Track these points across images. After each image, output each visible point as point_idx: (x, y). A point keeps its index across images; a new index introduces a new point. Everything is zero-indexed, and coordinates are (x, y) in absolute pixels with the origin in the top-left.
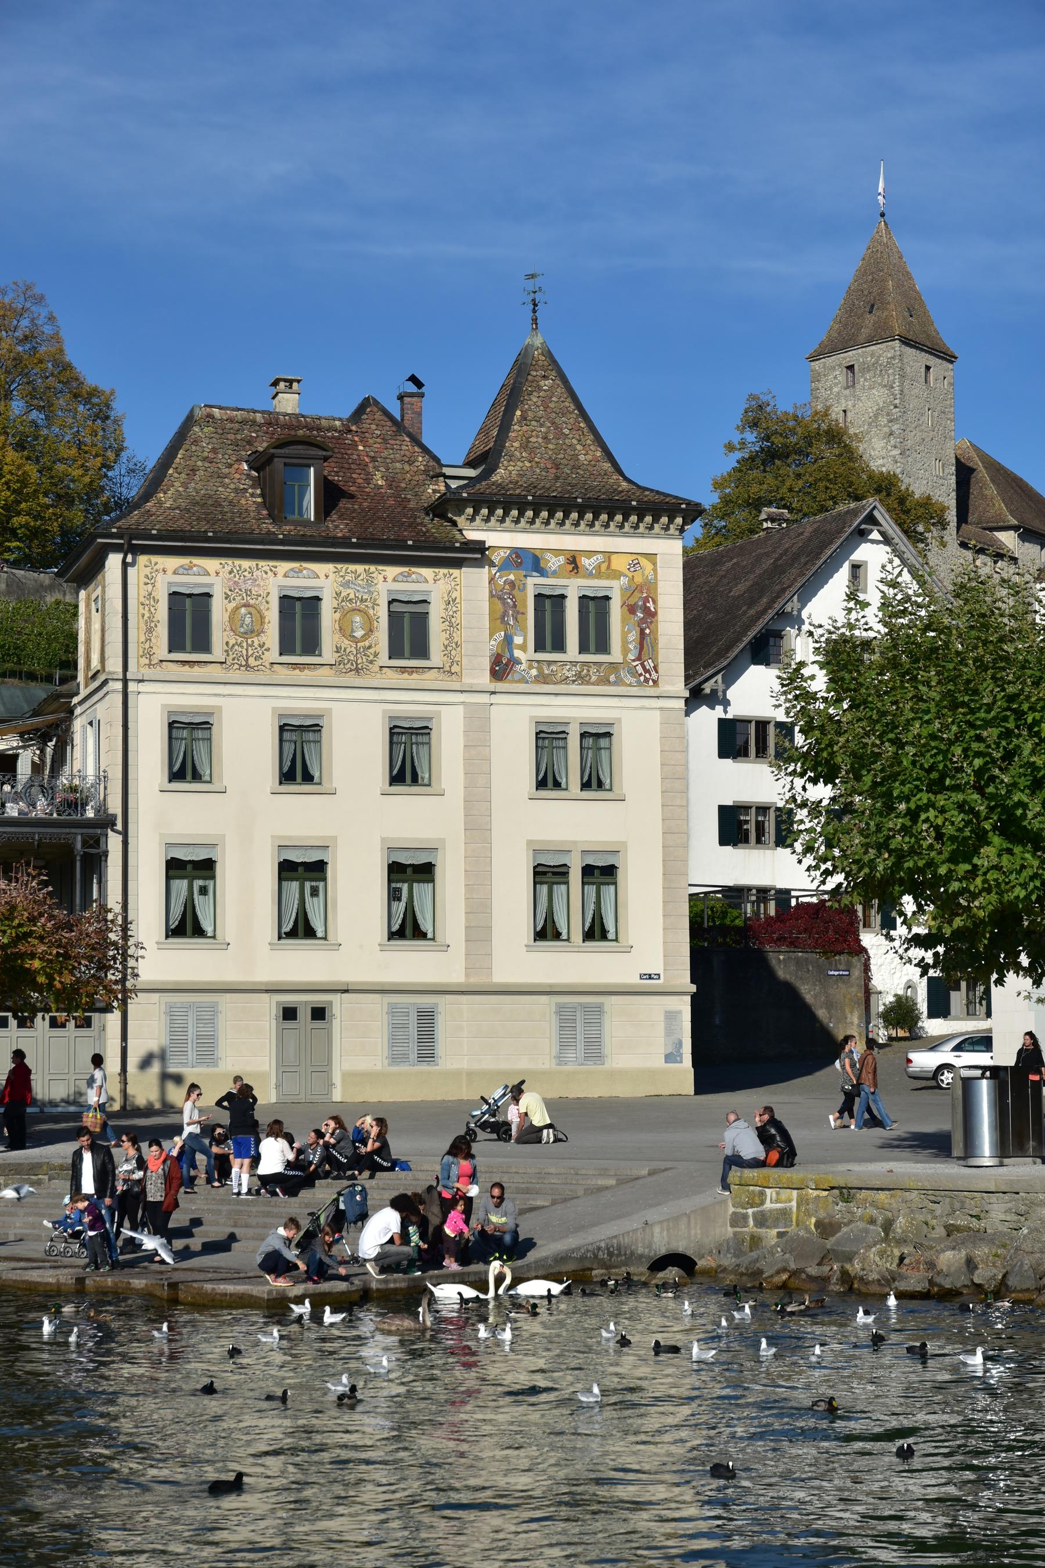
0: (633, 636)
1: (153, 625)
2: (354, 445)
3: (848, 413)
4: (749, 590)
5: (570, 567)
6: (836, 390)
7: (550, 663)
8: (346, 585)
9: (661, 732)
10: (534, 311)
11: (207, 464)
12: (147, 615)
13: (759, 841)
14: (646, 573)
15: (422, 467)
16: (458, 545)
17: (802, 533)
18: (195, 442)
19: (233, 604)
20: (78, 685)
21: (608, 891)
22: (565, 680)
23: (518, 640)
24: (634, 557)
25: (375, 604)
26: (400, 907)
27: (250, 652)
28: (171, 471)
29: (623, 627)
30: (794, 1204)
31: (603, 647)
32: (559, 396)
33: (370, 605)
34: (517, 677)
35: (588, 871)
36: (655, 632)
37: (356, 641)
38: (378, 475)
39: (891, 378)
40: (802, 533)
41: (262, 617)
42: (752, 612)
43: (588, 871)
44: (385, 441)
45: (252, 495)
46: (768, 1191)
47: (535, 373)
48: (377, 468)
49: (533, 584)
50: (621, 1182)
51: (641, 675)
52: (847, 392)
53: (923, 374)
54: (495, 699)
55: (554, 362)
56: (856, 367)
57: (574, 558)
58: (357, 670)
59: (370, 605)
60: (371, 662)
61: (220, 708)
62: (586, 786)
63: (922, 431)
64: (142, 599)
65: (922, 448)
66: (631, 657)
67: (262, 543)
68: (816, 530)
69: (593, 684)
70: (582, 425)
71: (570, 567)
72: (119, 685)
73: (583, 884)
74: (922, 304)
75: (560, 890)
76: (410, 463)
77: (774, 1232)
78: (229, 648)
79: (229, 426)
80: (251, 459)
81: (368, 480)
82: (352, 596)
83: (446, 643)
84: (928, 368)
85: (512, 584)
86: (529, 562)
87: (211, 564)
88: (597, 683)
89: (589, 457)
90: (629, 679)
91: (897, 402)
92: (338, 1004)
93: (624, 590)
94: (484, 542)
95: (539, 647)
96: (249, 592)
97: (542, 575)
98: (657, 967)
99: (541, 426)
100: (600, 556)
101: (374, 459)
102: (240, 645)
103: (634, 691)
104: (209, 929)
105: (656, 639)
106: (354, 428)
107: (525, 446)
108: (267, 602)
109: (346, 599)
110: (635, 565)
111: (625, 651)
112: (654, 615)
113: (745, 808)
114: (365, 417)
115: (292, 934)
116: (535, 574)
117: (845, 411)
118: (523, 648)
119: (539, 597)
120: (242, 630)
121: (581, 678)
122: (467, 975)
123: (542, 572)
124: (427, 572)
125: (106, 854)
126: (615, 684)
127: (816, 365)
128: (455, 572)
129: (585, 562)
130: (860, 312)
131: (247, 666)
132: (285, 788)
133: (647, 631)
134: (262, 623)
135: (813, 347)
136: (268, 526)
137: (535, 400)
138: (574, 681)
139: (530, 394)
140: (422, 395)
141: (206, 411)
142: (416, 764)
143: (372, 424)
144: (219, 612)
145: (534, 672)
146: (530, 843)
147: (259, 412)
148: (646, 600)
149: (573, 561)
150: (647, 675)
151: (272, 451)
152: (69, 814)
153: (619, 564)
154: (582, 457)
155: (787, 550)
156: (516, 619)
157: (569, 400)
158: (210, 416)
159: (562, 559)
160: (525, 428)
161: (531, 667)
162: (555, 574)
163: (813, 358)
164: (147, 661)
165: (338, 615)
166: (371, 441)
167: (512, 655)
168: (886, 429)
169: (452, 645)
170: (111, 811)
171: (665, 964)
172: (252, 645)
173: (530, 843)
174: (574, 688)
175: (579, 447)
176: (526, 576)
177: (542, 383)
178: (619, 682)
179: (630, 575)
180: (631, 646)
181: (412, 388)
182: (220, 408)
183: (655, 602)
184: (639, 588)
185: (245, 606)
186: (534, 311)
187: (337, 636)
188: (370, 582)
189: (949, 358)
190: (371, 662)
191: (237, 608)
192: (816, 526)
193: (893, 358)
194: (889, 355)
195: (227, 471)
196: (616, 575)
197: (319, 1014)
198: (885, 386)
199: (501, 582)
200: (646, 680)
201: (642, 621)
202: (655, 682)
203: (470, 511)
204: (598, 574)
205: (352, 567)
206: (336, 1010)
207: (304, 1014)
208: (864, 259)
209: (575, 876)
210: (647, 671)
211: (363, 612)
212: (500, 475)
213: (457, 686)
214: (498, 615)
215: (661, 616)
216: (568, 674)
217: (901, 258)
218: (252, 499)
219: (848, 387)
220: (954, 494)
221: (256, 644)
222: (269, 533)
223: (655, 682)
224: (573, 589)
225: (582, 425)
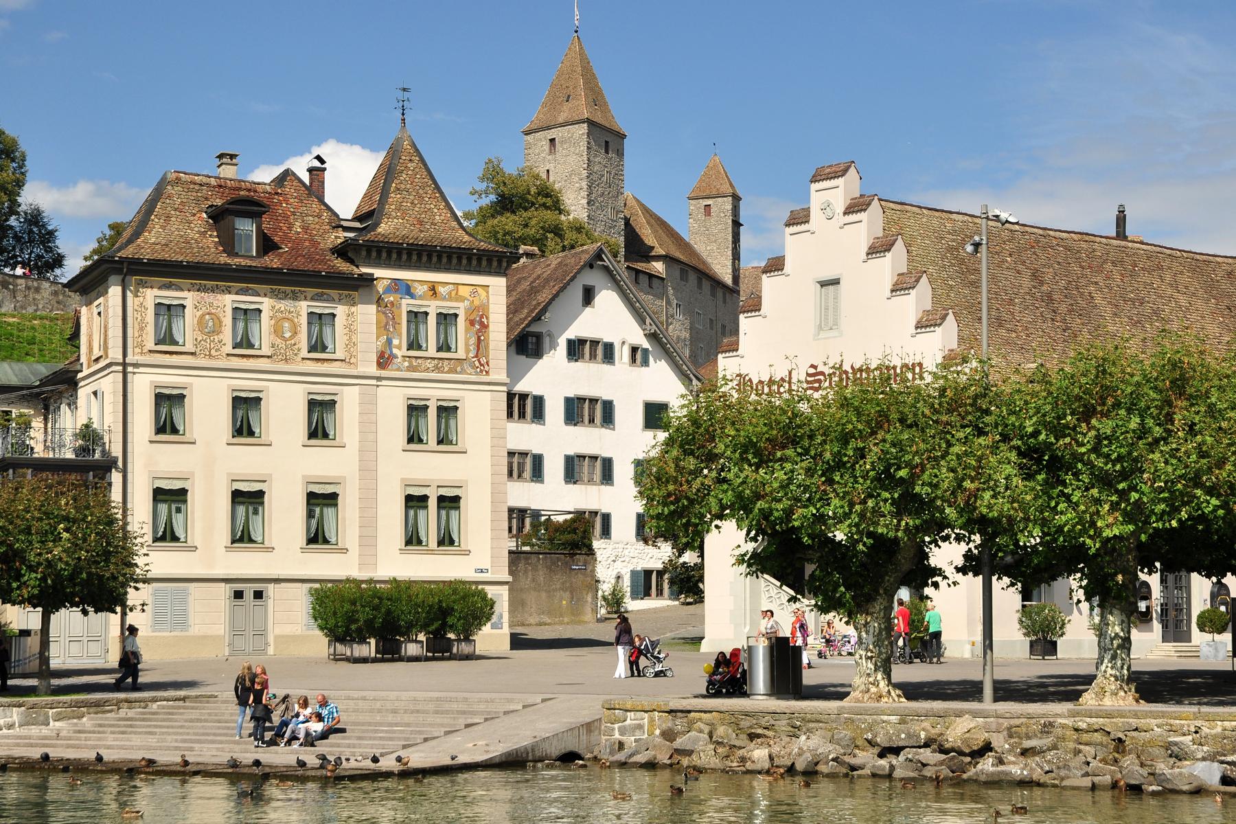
0: (473, 340)
1: (144, 325)
5: (431, 293)
9: (491, 406)
10: (403, 114)
11: (178, 213)
12: (139, 318)
14: (482, 298)
15: (327, 220)
16: (356, 276)
17: (549, 265)
18: (169, 197)
19: (200, 313)
20: (82, 364)
21: (454, 514)
22: (427, 370)
23: (396, 342)
24: (474, 287)
25: (299, 315)
26: (314, 522)
27: (212, 346)
28: (153, 217)
29: (466, 335)
30: (646, 721)
32: (421, 174)
33: (295, 315)
34: (395, 367)
35: (441, 499)
36: (487, 339)
37: (286, 340)
39: (582, 148)
40: (549, 265)
41: (221, 322)
43: (441, 499)
45: (211, 236)
46: (628, 714)
47: (404, 158)
49: (406, 304)
50: (524, 707)
51: (478, 367)
55: (417, 150)
57: (434, 287)
58: (286, 359)
59: (295, 315)
60: (296, 355)
61: (191, 384)
62: (440, 442)
64: (136, 307)
66: (471, 355)
68: (560, 263)
69: (446, 373)
70: (437, 195)
71: (431, 293)
72: (120, 368)
73: (439, 507)
75: (421, 513)
77: (633, 738)
78: (197, 343)
79: (192, 186)
80: (210, 210)
81: (290, 228)
82: (283, 309)
83: (347, 342)
88: (450, 371)
89: (442, 218)
90: (470, 370)
92: (271, 589)
93: (467, 310)
94: (373, 274)
96: (211, 305)
97: (412, 298)
98: (486, 564)
102: (205, 341)
104: (333, 540)
105: (488, 344)
106: (279, 191)
108: (224, 312)
109: (279, 311)
111: (468, 351)
112: (486, 327)
114: (286, 183)
115: (163, 539)
116: (407, 297)
117: (548, 171)
118: (399, 347)
120: (206, 330)
121: (437, 369)
122: (360, 569)
123: (412, 296)
125: (110, 484)
126: (460, 373)
127: (528, 137)
129: (442, 290)
130: (560, 100)
131: (210, 355)
132: (236, 440)
133: (482, 338)
135: (525, 128)
136: (224, 259)
137: (405, 176)
138: (433, 371)
139: (402, 172)
140: (324, 169)
141: (174, 176)
142: (326, 425)
143: (289, 188)
145: (406, 364)
146: (402, 480)
147: (212, 177)
148: (482, 317)
149: (433, 289)
150: (482, 368)
151: (227, 206)
152: (84, 456)
153: (464, 291)
154: (437, 217)
155: (539, 277)
156: (394, 327)
157: (428, 177)
158: (178, 179)
159: (425, 287)
160: (399, 196)
162: (421, 298)
163: (527, 133)
164: (140, 351)
165: (273, 322)
166: (292, 200)
167: (391, 352)
168: (577, 185)
169: (351, 344)
170: (114, 454)
171: (492, 563)
172: (213, 341)
173: (402, 480)
175: (436, 211)
176: (401, 298)
177: (409, 165)
178: (463, 372)
179: (471, 299)
181: (317, 164)
182: (185, 173)
183: (487, 318)
184: (477, 309)
185: (209, 314)
186: (403, 114)
187: (272, 336)
190: (296, 355)
191: (203, 316)
192: (559, 260)
193: (583, 134)
194: (581, 133)
195: (192, 218)
196: (461, 299)
197: (258, 595)
198: (577, 154)
200: (481, 371)
201: (479, 331)
202: (487, 372)
204: (450, 299)
206: (271, 593)
207: (249, 595)
209: (432, 503)
210: (482, 365)
212: (384, 228)
214: (383, 324)
215: (491, 328)
216: (428, 366)
217: (588, 63)
218: (212, 239)
221: (216, 340)
222: (226, 264)
223: (487, 372)
224: (433, 308)
225: (437, 195)
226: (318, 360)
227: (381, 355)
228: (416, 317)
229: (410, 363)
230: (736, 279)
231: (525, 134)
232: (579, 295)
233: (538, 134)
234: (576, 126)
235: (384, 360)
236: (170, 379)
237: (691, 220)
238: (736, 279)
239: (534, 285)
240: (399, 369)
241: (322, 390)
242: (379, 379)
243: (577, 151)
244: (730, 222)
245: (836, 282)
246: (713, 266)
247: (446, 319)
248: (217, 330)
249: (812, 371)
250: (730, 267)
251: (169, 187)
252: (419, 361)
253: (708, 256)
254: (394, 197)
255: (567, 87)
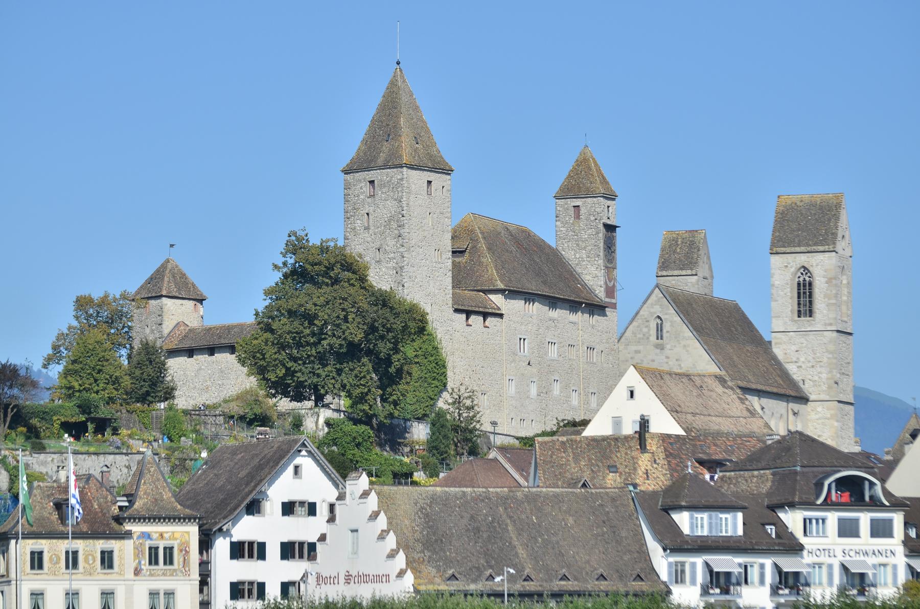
0: (182, 560)
2: (87, 493)
3: (370, 215)
4: (247, 476)
6: (362, 197)
7: (153, 570)
8: (87, 546)
13: (249, 597)
17: (273, 447)
18: (35, 496)
22: (159, 575)
23: (143, 562)
31: (171, 563)
37: (90, 565)
38: (95, 504)
42: (247, 490)
44: (97, 491)
48: (95, 501)
52: (370, 200)
53: (426, 188)
54: (136, 582)
56: (376, 182)
63: (424, 230)
65: (423, 243)
66: (181, 567)
67: (60, 534)
72: (15, 582)
74: (428, 131)
76: (106, 498)
84: (429, 182)
85: (141, 544)
86: (147, 536)
87: (43, 541)
90: (180, 574)
91: (404, 212)
93: (178, 545)
94: (131, 531)
95: (150, 563)
96: (55, 550)
99: (151, 485)
100: (170, 533)
101: (94, 498)
103: (182, 578)
107: (145, 494)
110: (182, 536)
113: (243, 583)
118: (145, 565)
119: (150, 548)
121: (164, 574)
123: (151, 539)
124: (113, 541)
127: (348, 177)
128: (122, 541)
129: (165, 535)
134: (60, 560)
135: (345, 162)
144: (46, 558)
145: (148, 573)
149: (161, 535)
153: (176, 535)
154: (164, 497)
156: (142, 555)
159: (158, 535)
161: (147, 571)
162: (155, 540)
163: (346, 172)
168: (396, 232)
169: (121, 565)
174: (162, 578)
178: (177, 575)
180: (181, 563)
184: (184, 543)
185: (55, 554)
188: (94, 545)
189: (446, 171)
191: (52, 556)
192: (279, 444)
194: (399, 177)
196: (176, 539)
199: (137, 543)
200: (186, 575)
201: (185, 554)
203: (127, 520)
204: (170, 539)
205: (88, 541)
208: (384, 96)
211: (92, 555)
213: (122, 578)
217: (412, 95)
218: (55, 516)
219: (371, 196)
220: (450, 274)
222: (62, 531)
223: (189, 575)
224: (161, 545)
226: (105, 574)
227: (136, 569)
228: (153, 551)
229: (150, 572)
230: (610, 292)
231: (345, 174)
232: (291, 469)
233: (358, 174)
234: (395, 170)
235: (137, 572)
236: (37, 586)
237: (558, 223)
238: (610, 292)
239: (262, 462)
240: (145, 576)
241: (108, 586)
242: (134, 581)
243: (396, 197)
244: (601, 226)
245: (357, 531)
246: (583, 277)
247: (169, 551)
248: (58, 562)
249: (347, 574)
250: (602, 278)
251: (35, 491)
252: (155, 571)
253: (577, 265)
254: (142, 487)
255: (388, 125)
